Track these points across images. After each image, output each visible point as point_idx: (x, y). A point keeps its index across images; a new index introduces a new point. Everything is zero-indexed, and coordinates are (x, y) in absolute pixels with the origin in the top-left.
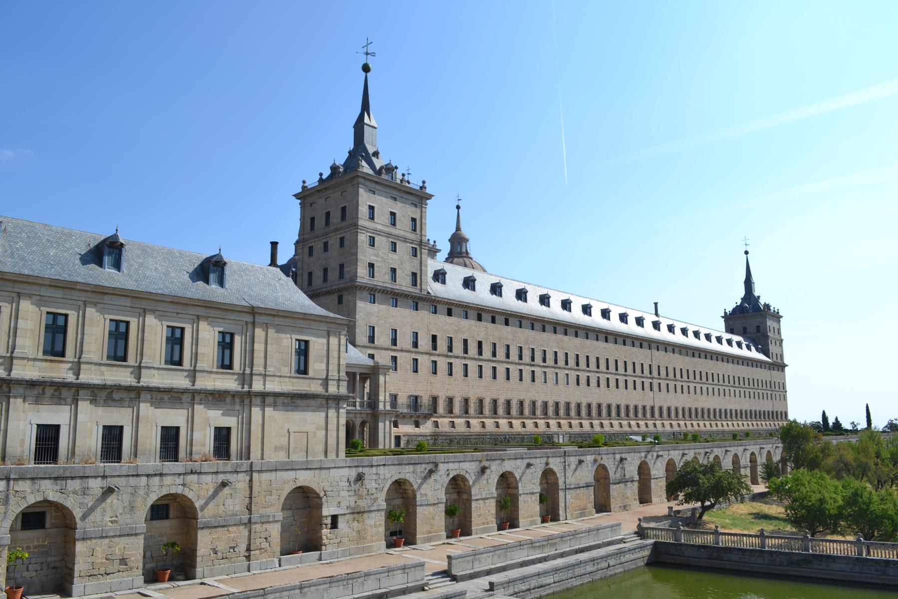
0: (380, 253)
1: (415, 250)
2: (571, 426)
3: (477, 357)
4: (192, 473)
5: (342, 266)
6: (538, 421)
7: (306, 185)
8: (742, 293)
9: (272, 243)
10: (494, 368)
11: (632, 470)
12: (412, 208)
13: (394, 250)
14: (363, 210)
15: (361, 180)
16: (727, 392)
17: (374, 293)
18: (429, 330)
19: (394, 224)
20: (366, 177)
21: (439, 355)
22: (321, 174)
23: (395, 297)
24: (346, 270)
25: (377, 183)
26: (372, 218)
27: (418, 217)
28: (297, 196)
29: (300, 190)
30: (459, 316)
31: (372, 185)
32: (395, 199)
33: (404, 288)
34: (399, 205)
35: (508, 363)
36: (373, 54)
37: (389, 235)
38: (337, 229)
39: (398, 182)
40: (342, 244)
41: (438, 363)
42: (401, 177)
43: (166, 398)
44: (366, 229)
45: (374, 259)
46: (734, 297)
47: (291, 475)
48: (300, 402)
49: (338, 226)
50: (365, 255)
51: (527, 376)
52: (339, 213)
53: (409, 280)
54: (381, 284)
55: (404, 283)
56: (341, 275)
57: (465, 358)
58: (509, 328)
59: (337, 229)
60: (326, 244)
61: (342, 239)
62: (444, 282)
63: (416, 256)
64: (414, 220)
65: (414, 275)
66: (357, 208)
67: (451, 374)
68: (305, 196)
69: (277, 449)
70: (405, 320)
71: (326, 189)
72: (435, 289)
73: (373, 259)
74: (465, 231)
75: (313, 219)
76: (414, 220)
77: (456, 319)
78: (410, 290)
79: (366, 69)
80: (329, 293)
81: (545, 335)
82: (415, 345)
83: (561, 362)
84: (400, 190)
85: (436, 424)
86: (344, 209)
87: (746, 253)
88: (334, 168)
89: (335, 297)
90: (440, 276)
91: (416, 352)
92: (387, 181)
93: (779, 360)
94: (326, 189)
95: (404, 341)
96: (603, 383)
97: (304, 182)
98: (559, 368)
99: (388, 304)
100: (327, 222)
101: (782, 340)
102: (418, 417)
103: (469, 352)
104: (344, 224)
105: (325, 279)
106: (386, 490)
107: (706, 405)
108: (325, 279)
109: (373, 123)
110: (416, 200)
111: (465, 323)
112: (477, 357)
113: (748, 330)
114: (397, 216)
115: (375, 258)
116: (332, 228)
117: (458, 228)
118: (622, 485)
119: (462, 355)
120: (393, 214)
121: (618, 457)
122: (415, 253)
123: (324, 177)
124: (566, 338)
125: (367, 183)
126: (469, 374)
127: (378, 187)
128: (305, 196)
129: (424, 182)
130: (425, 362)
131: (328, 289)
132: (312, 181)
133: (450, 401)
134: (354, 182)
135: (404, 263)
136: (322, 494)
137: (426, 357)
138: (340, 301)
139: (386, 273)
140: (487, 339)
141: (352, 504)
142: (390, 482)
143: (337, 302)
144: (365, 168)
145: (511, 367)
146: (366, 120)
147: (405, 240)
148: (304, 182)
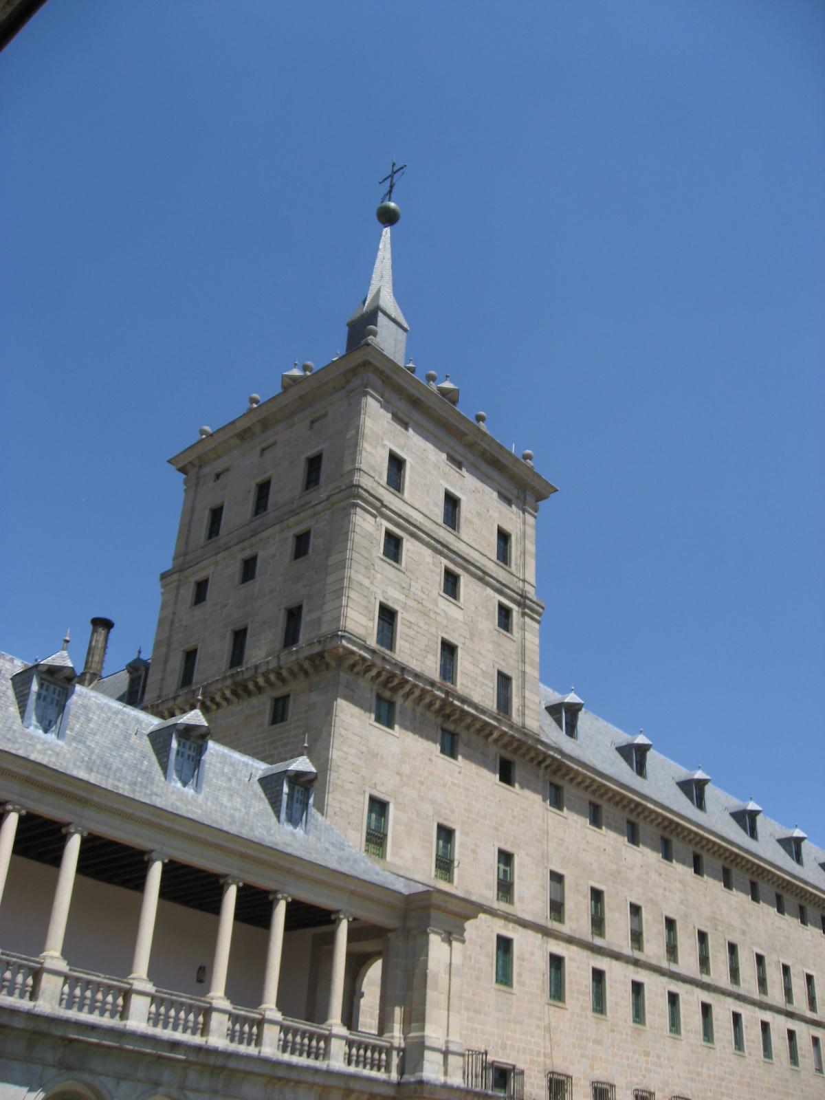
0: (415, 588)
3: (665, 964)
10: (706, 1009)
15: (373, 378)
23: (453, 727)
24: (306, 618)
31: (403, 406)
32: (459, 465)
35: (739, 997)
41: (569, 966)
52: (300, 471)
64: (504, 537)
73: (395, 598)
89: (263, 704)
103: (646, 945)
115: (401, 597)
119: (626, 948)
120: (452, 502)
126: (648, 1017)
127: (416, 416)
130: (531, 952)
137: (534, 938)
140: (686, 916)
143: (267, 717)
145: (746, 1012)
147: (482, 577)
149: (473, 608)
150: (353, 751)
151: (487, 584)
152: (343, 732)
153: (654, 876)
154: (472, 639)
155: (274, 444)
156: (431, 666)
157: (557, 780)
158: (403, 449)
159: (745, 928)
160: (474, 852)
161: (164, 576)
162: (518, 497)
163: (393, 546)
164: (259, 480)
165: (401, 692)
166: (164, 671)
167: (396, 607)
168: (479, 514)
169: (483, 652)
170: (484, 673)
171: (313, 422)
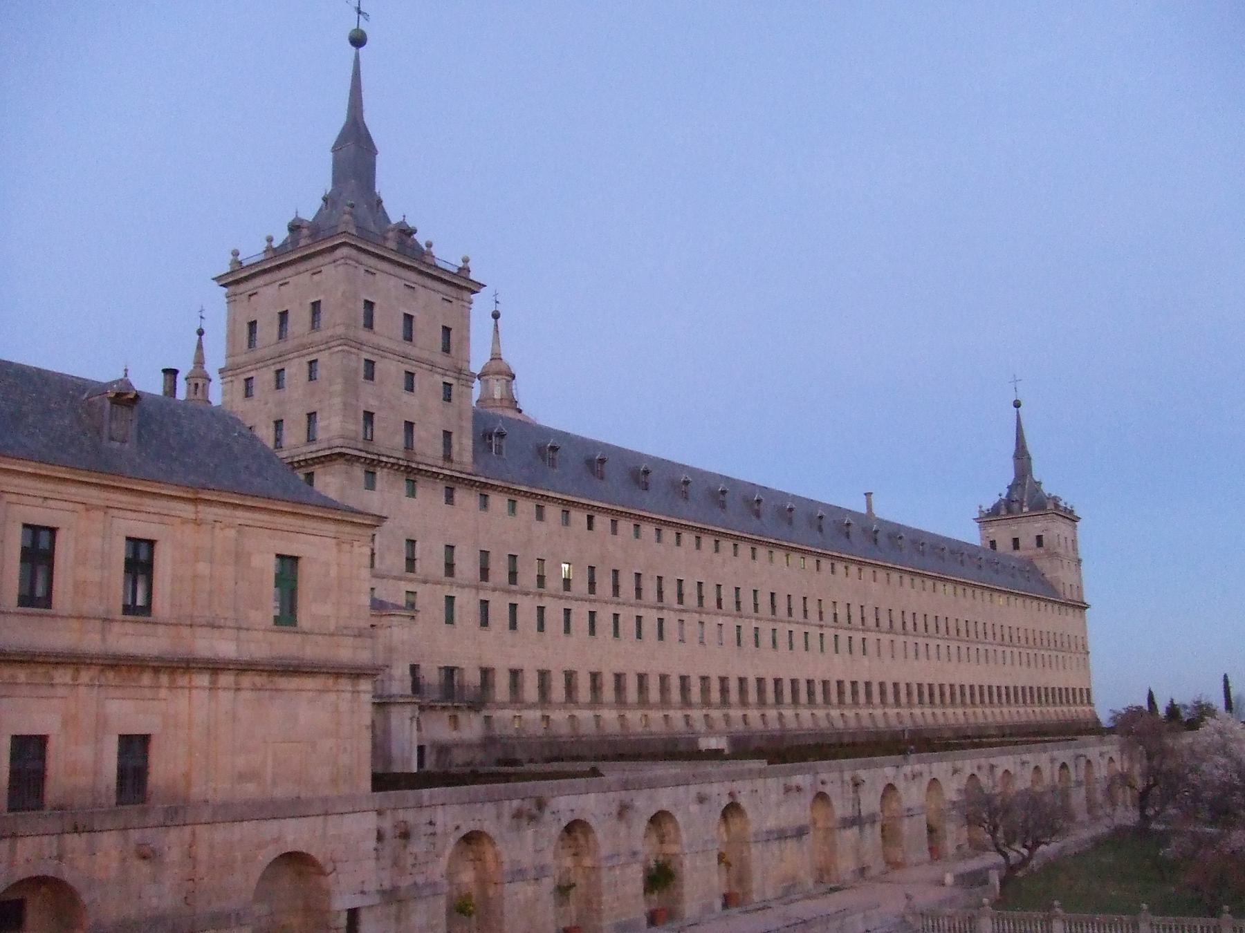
1: (448, 386)
2: (727, 718)
3: (561, 593)
4: (76, 830)
5: (311, 416)
6: (671, 713)
7: (240, 258)
8: (1010, 477)
9: (165, 371)
11: (870, 802)
13: (410, 387)
16: (991, 654)
21: (494, 590)
22: (270, 240)
24: (320, 423)
38: (304, 347)
43: (22, 675)
44: (360, 345)
46: (996, 483)
47: (270, 829)
48: (283, 682)
49: (305, 340)
51: (650, 627)
52: (307, 315)
57: (541, 595)
60: (279, 372)
67: (513, 625)
68: (238, 279)
69: (242, 777)
73: (372, 404)
78: (440, 463)
82: (450, 568)
83: (710, 602)
85: (488, 719)
86: (316, 306)
87: (1017, 405)
88: (295, 228)
91: (451, 584)
93: (1075, 598)
95: (430, 560)
96: (782, 640)
97: (236, 253)
98: (707, 613)
101: (1079, 561)
102: (457, 707)
104: (317, 336)
106: (448, 852)
107: (957, 680)
112: (561, 593)
113: (1021, 544)
116: (290, 344)
118: (856, 829)
121: (847, 776)
123: (275, 244)
125: (364, 258)
129: (466, 261)
130: (467, 602)
132: (253, 251)
133: (515, 674)
136: (329, 868)
141: (387, 885)
142: (452, 841)
148: (236, 253)
156: (400, 439)
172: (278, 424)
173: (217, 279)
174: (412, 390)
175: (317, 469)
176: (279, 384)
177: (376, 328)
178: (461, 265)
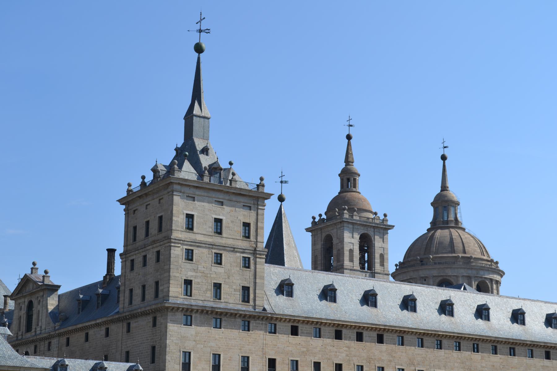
0: (201, 268)
5: (157, 283)
7: (132, 188)
9: (107, 250)
12: (246, 212)
14: (179, 220)
15: (176, 187)
17: (189, 315)
18: (264, 354)
19: (220, 233)
20: (184, 183)
22: (143, 178)
23: (218, 317)
24: (161, 288)
25: (197, 187)
26: (190, 227)
27: (251, 220)
28: (122, 201)
29: (125, 195)
30: (308, 334)
31: (191, 191)
32: (222, 204)
33: (231, 306)
34: (227, 209)
36: (208, 31)
37: (212, 246)
38: (154, 242)
39: (228, 184)
40: (158, 260)
42: (230, 177)
45: (191, 274)
50: (180, 270)
53: (239, 295)
54: (201, 303)
55: (231, 300)
56: (157, 295)
58: (383, 347)
59: (154, 242)
60: (145, 257)
61: (158, 253)
62: (290, 294)
63: (249, 267)
64: (246, 225)
65: (246, 290)
66: (171, 219)
68: (130, 201)
70: (231, 342)
71: (146, 195)
72: (279, 305)
73: (190, 275)
74: (454, 192)
75: (135, 228)
76: (246, 225)
77: (304, 338)
79: (199, 49)
80: (145, 314)
81: (442, 352)
84: (228, 192)
86: (161, 218)
89: (150, 319)
90: (285, 288)
92: (217, 183)
94: (146, 195)
97: (129, 185)
99: (209, 325)
100: (147, 234)
104: (160, 236)
105: (143, 299)
108: (143, 299)
109: (206, 112)
110: (250, 202)
111: (317, 343)
114: (224, 222)
116: (151, 239)
117: (444, 188)
120: (218, 221)
122: (246, 264)
124: (477, 356)
127: (198, 192)
128: (130, 201)
129: (262, 179)
131: (143, 309)
132: (136, 185)
134: (169, 190)
135: (232, 275)
138: (154, 325)
139: (207, 290)
144: (188, 172)
146: (196, 110)
147: (234, 250)
148: (129, 185)
149: (229, 265)
150: (174, 338)
151: (237, 252)
152: (170, 333)
153: (329, 348)
154: (228, 278)
155: (149, 204)
156: (210, 295)
157: (273, 322)
158: (192, 211)
159: (391, 359)
160: (229, 360)
161: (121, 255)
162: (254, 204)
163: (189, 255)
164: (146, 220)
165: (194, 312)
166: (124, 296)
167: (191, 279)
168: (232, 222)
169: (234, 281)
170: (235, 290)
171: (160, 200)
172: (144, 287)
173: (119, 201)
174: (220, 264)
175: (158, 315)
176: (145, 264)
177: (195, 230)
178: (258, 182)
